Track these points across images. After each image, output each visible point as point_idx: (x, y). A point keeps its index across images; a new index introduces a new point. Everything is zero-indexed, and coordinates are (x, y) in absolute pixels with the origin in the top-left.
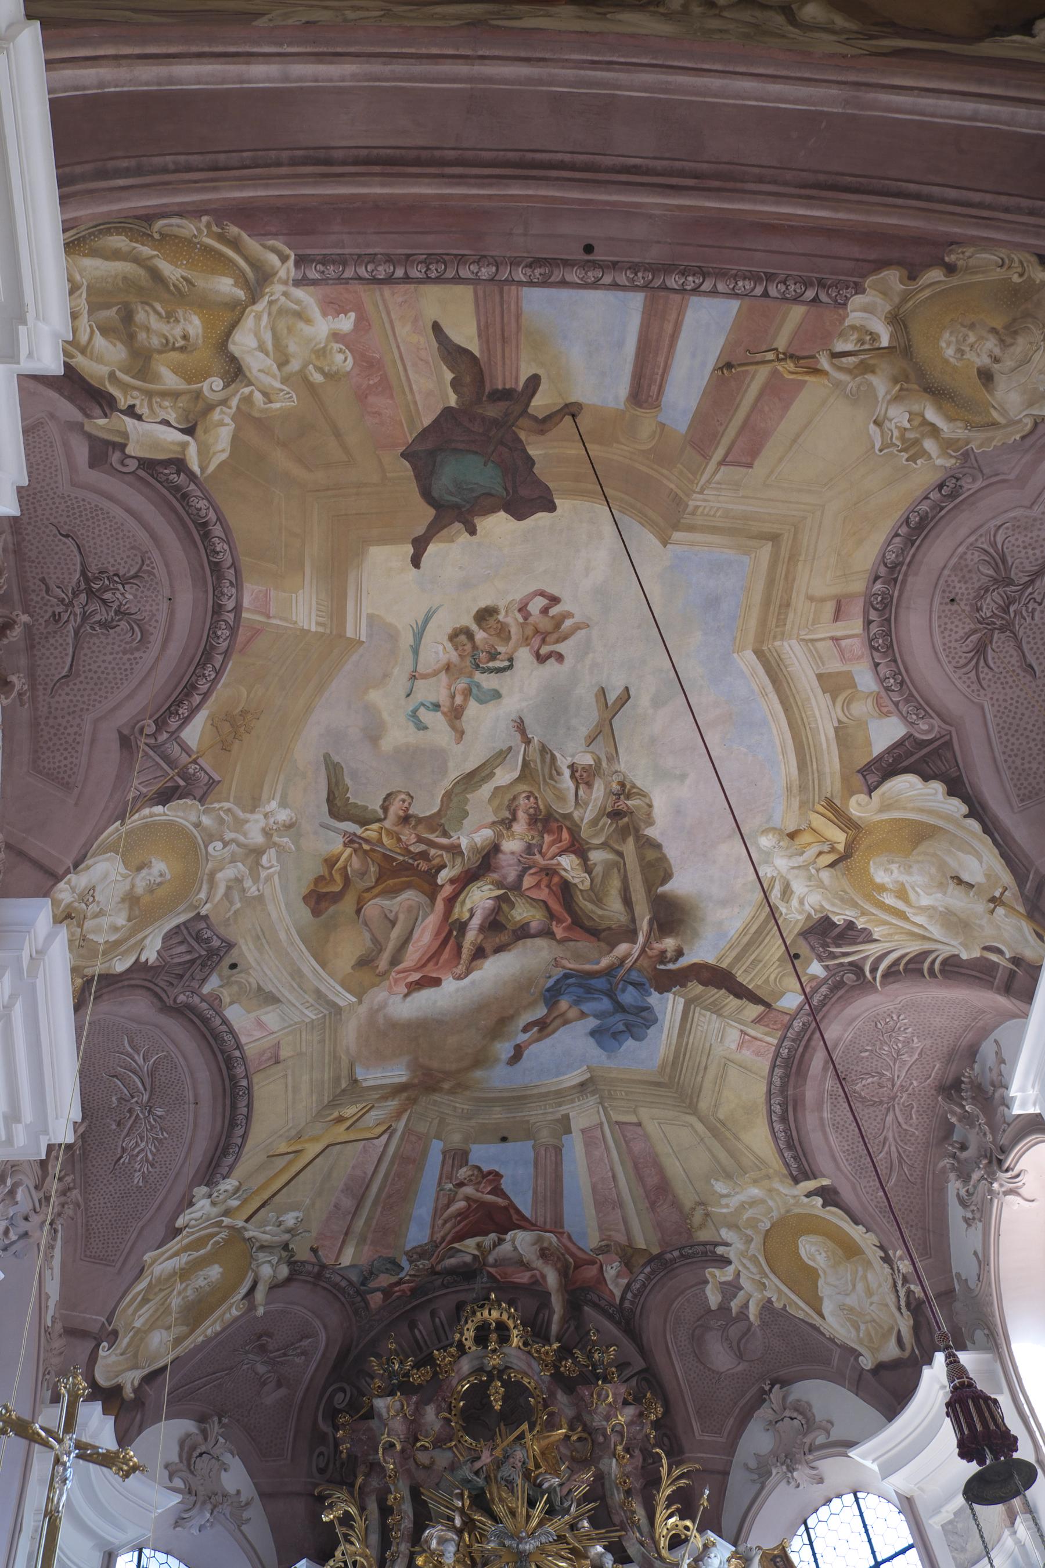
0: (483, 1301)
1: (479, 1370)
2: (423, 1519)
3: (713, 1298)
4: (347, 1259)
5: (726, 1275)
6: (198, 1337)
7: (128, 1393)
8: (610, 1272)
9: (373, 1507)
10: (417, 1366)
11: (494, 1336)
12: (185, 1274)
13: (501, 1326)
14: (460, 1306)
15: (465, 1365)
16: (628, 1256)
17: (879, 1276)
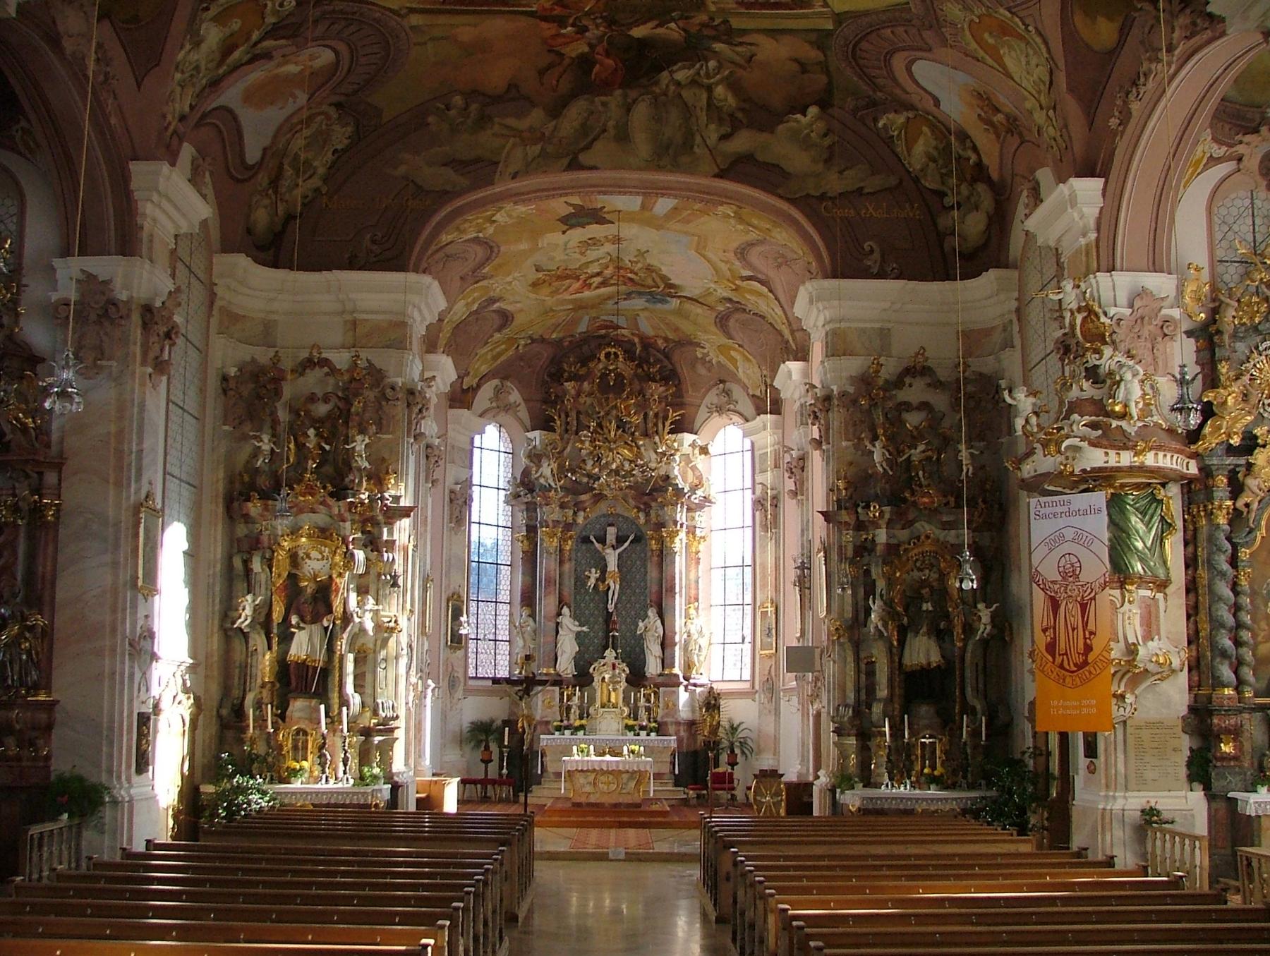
0: (609, 345)
1: (606, 368)
2: (581, 427)
3: (700, 356)
4: (554, 336)
5: (705, 351)
6: (499, 362)
7: (475, 385)
8: (660, 342)
9: (563, 416)
10: (581, 367)
11: (612, 356)
12: (491, 350)
13: (615, 353)
14: (600, 345)
15: (601, 366)
16: (666, 339)
17: (757, 369)
